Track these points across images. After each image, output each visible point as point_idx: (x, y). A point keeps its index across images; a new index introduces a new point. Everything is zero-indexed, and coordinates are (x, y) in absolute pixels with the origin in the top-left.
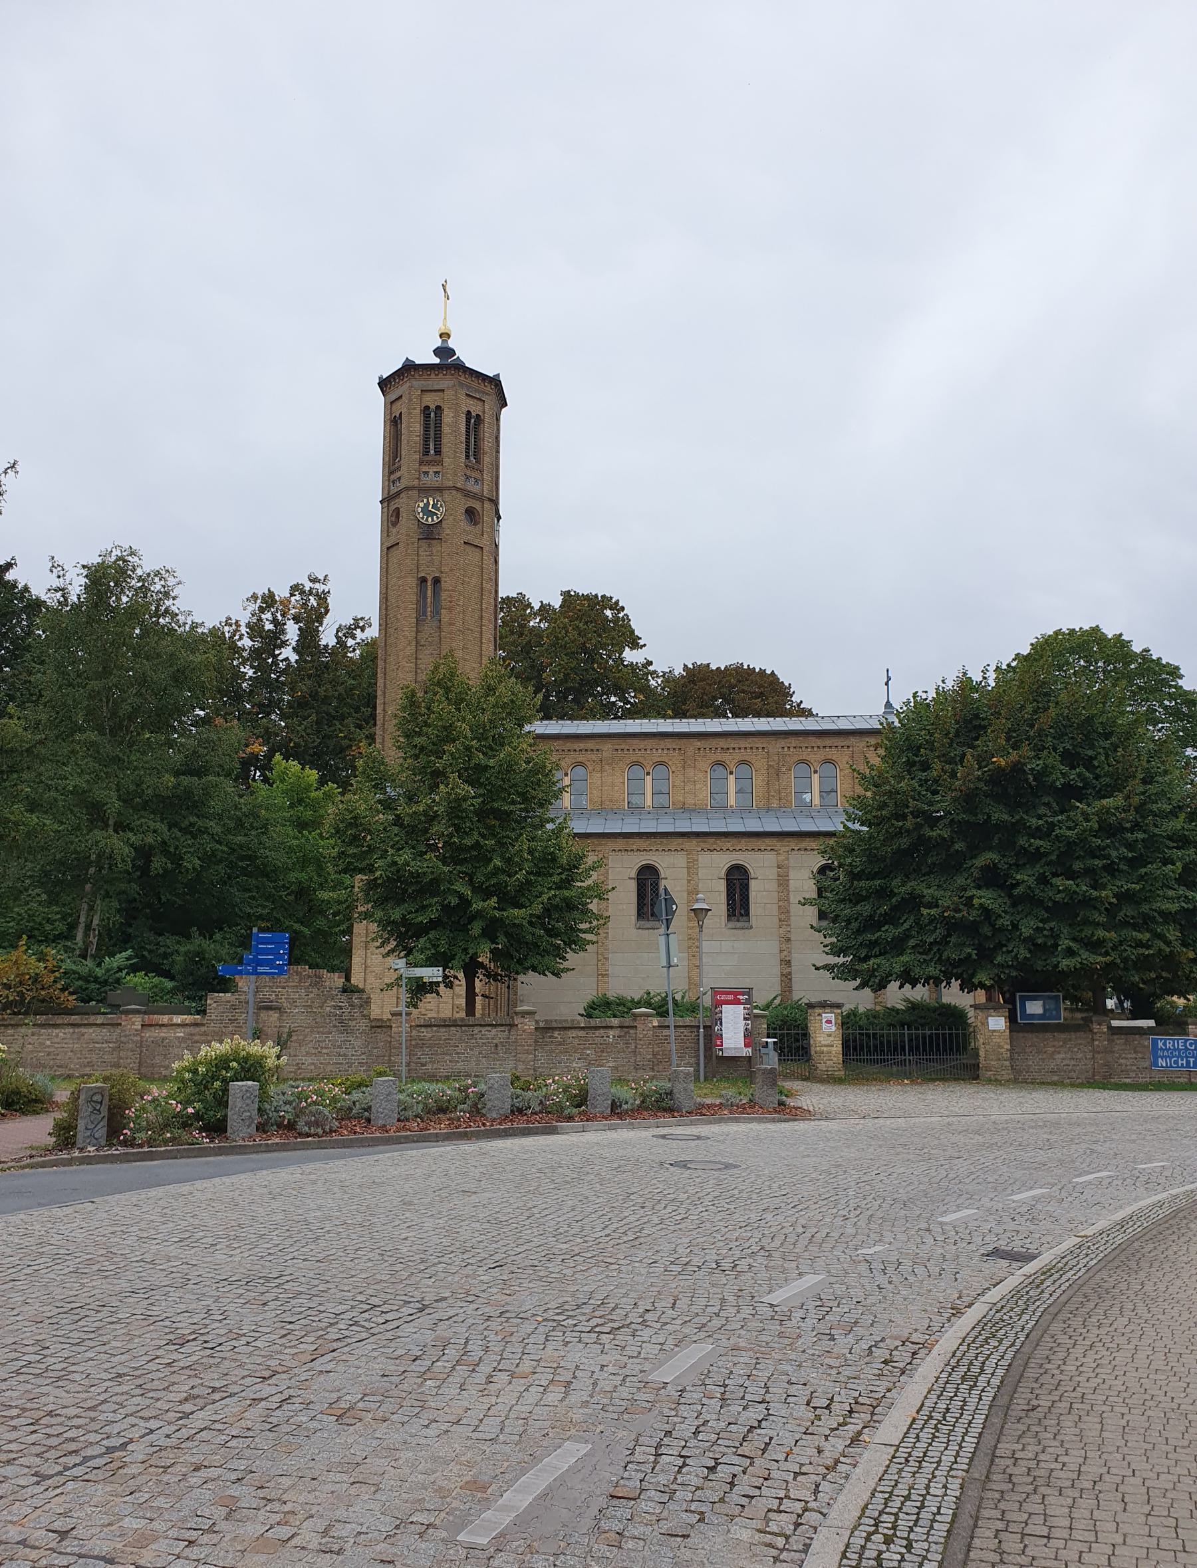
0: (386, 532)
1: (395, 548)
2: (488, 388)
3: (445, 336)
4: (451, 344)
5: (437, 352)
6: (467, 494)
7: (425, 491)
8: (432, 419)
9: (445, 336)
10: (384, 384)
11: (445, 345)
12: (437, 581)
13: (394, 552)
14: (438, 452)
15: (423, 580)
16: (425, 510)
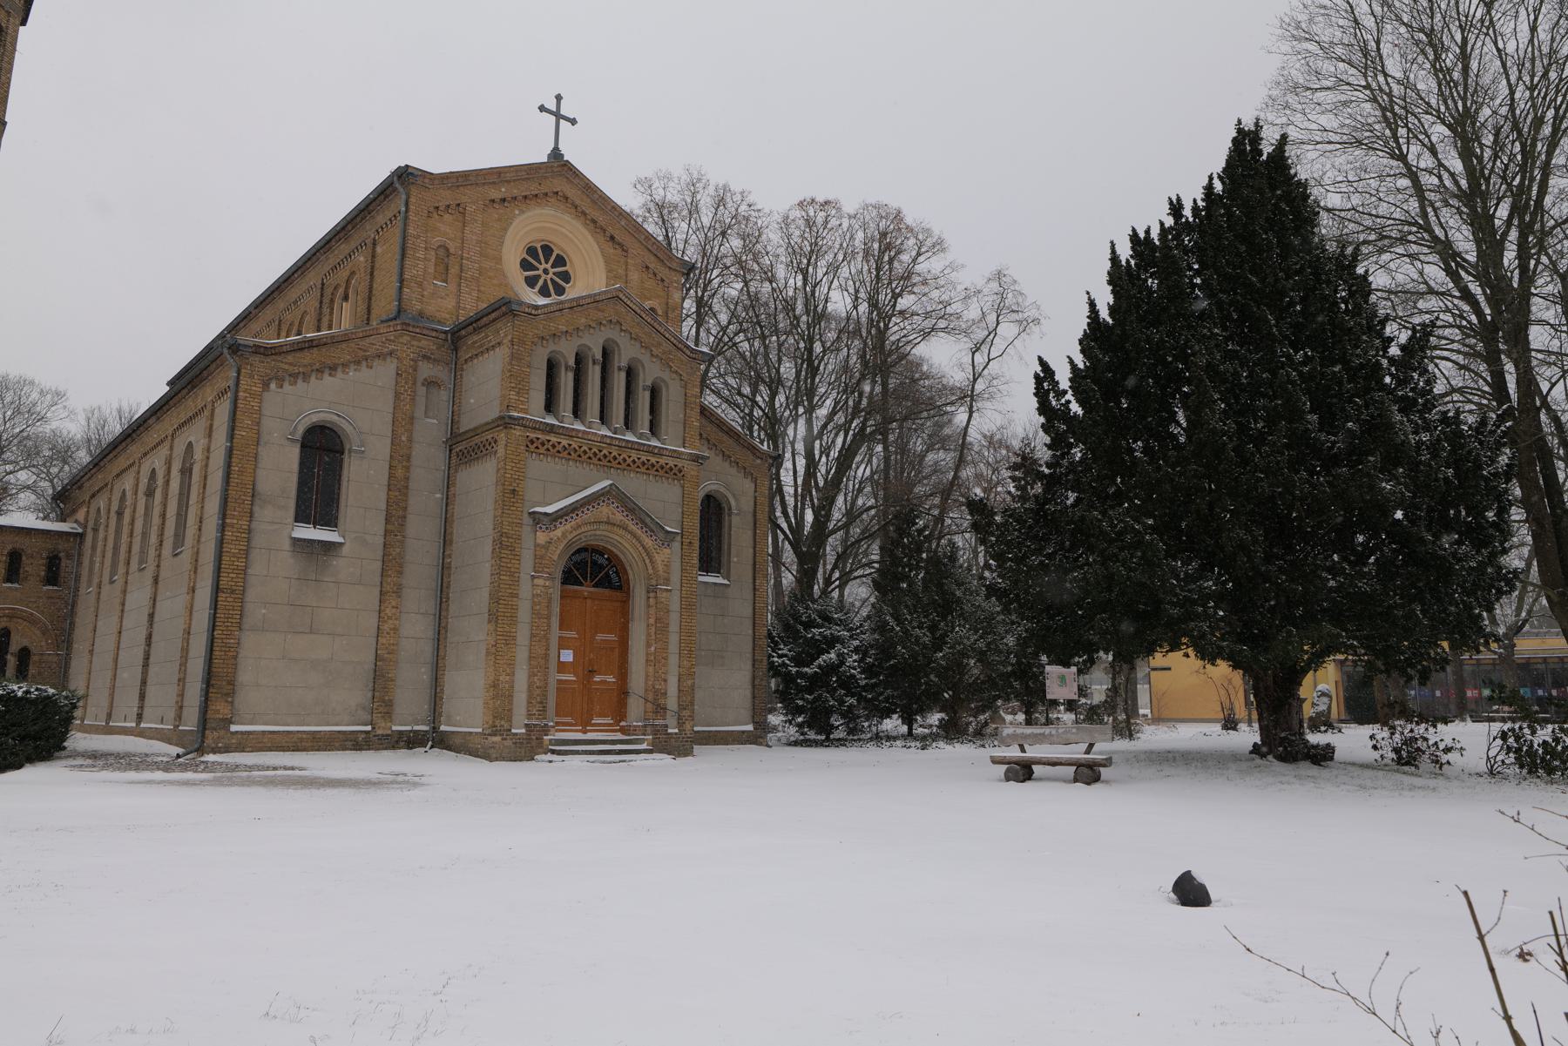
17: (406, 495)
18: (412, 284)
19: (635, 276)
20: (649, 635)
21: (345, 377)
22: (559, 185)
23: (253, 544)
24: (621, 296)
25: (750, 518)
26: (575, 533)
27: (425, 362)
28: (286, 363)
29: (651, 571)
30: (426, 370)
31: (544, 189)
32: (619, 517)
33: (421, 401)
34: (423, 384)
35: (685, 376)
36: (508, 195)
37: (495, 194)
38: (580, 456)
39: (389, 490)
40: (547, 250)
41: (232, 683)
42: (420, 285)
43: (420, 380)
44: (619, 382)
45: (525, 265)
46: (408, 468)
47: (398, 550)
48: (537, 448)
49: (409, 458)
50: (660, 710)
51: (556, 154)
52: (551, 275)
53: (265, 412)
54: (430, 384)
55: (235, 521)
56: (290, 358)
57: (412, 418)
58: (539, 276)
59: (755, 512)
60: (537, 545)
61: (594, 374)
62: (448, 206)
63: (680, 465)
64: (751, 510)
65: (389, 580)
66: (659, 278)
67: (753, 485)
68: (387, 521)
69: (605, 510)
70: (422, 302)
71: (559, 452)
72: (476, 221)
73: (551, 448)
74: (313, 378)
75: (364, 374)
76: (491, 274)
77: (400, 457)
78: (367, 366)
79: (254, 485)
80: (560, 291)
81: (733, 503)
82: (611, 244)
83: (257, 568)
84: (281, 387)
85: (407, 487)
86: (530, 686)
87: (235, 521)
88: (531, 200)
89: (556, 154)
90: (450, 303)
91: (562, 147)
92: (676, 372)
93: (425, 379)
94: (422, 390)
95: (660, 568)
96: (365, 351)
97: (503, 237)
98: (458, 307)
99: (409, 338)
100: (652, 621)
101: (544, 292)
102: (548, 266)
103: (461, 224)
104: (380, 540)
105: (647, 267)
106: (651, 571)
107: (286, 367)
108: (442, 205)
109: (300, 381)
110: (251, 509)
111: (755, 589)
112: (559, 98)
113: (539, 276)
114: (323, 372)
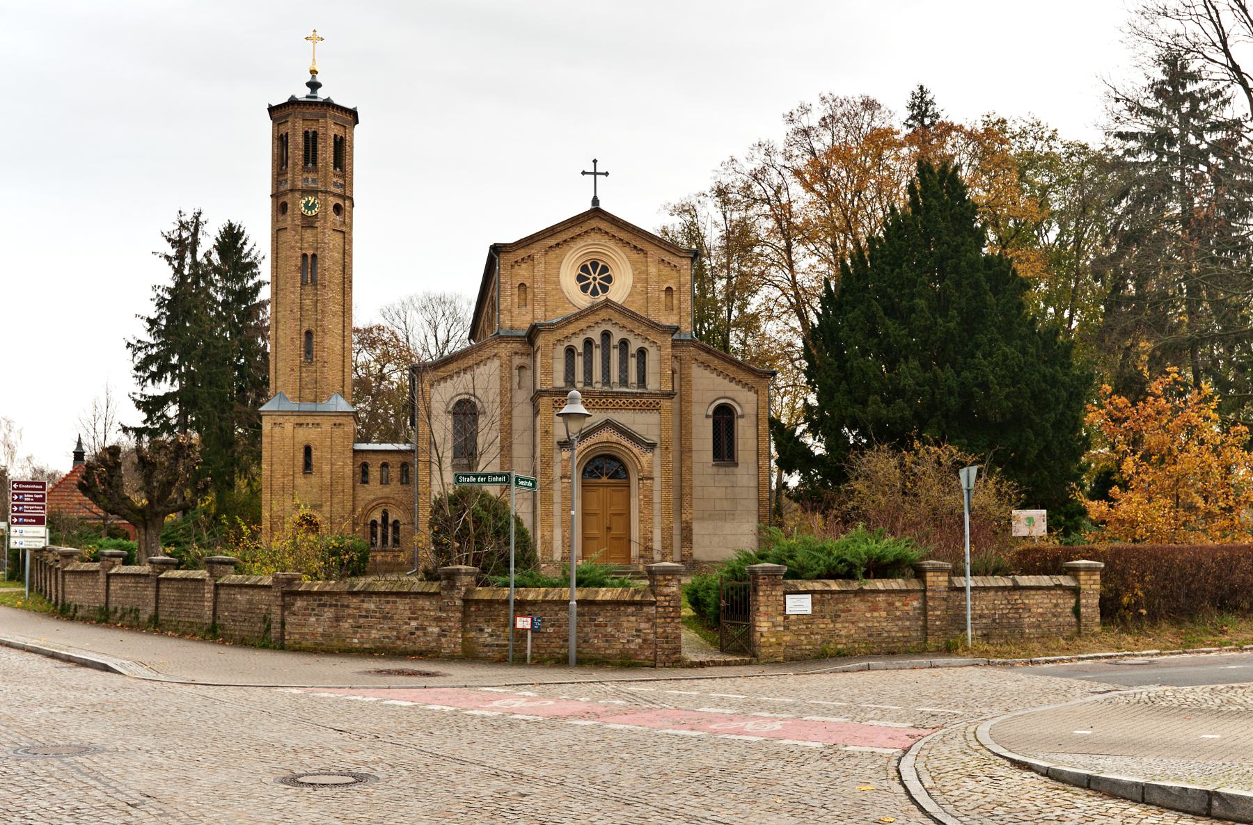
0: (275, 220)
3: (314, 72)
4: (319, 79)
5: (308, 84)
6: (335, 195)
7: (305, 192)
8: (311, 140)
9: (314, 72)
10: (272, 110)
12: (314, 256)
14: (315, 163)
15: (305, 256)
16: (306, 205)
17: (511, 434)
19: (653, 270)
20: (640, 505)
22: (594, 223)
25: (754, 418)
30: (517, 361)
31: (584, 229)
32: (615, 437)
33: (516, 379)
37: (552, 242)
40: (595, 264)
42: (510, 311)
43: (514, 366)
44: (615, 355)
45: (580, 278)
46: (511, 419)
49: (510, 413)
50: (648, 549)
51: (595, 201)
54: (521, 368)
56: (442, 369)
61: (597, 355)
62: (523, 259)
64: (755, 412)
69: (607, 435)
77: (508, 414)
80: (605, 289)
86: (563, 536)
89: (595, 201)
94: (516, 372)
97: (559, 268)
98: (534, 319)
100: (641, 497)
101: (595, 293)
111: (758, 467)
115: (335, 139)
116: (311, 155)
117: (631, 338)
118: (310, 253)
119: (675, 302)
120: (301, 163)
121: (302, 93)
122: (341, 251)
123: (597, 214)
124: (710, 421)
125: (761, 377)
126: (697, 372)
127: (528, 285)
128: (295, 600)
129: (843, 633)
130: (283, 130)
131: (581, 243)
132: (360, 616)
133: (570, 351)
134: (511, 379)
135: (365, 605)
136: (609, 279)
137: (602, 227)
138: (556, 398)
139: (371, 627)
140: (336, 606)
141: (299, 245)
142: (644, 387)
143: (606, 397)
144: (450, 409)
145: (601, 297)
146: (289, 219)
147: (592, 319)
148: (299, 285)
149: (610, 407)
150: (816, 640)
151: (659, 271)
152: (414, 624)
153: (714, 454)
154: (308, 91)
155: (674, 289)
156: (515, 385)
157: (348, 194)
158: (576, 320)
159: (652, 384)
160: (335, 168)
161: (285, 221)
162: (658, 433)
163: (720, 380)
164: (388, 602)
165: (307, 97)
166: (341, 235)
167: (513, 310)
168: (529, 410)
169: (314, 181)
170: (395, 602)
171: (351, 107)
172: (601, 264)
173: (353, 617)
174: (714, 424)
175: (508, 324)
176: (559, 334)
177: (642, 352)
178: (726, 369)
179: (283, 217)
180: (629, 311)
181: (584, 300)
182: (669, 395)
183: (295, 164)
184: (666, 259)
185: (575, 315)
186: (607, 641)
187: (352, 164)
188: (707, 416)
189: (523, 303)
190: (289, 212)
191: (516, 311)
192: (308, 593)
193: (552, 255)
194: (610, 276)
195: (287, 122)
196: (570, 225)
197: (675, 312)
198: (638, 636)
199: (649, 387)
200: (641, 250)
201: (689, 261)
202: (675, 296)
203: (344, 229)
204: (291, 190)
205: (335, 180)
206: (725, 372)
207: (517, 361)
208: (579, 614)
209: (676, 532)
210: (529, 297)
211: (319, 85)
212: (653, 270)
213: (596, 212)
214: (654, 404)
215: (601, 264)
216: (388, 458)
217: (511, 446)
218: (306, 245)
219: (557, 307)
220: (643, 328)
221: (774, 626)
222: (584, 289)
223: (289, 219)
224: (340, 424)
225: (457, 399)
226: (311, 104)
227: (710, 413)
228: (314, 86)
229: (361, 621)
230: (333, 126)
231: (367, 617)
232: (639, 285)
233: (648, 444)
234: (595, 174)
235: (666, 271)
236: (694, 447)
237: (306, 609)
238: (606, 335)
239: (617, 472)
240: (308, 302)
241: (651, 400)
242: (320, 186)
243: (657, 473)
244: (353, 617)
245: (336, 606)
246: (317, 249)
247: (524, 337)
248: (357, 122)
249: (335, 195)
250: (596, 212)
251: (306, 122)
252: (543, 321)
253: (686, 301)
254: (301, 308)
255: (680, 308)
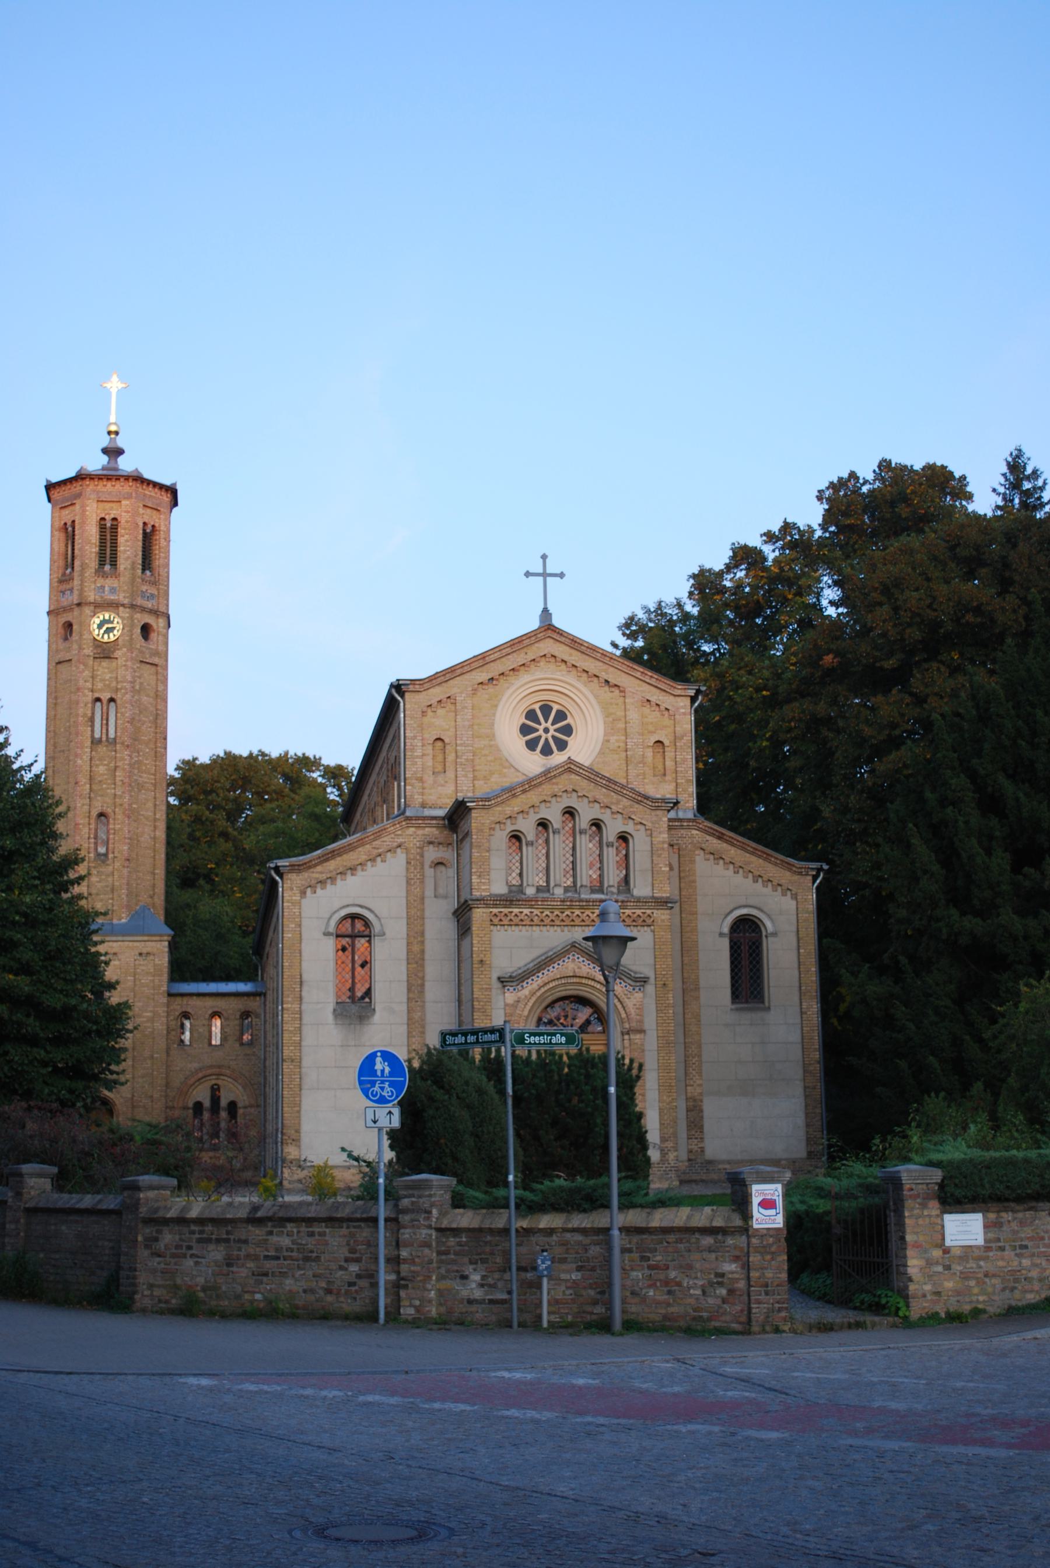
1: (66, 665)
2: (166, 498)
4: (121, 442)
5: (105, 451)
6: (143, 609)
8: (109, 532)
10: (50, 487)
11: (112, 445)
13: (62, 668)
14: (114, 563)
17: (423, 966)
18: (414, 781)
21: (364, 873)
22: (548, 646)
23: (304, 1021)
24: (572, 767)
26: (543, 990)
27: (431, 846)
28: (317, 872)
29: (624, 1015)
30: (432, 854)
31: (531, 657)
34: (431, 867)
35: (649, 825)
36: (494, 674)
37: (483, 676)
38: (542, 920)
39: (408, 963)
40: (546, 709)
41: (298, 1131)
42: (421, 780)
45: (525, 730)
46: (423, 942)
47: (419, 1014)
48: (501, 920)
49: (422, 934)
51: (546, 613)
52: (552, 732)
53: (303, 915)
55: (289, 1006)
56: (319, 868)
57: (423, 898)
58: (540, 737)
59: (798, 931)
60: (506, 1005)
63: (649, 912)
64: (794, 929)
65: (414, 1040)
66: (662, 708)
67: (794, 903)
68: (409, 990)
70: (423, 794)
71: (522, 920)
72: (466, 707)
73: (512, 918)
74: (339, 881)
75: (379, 867)
76: (486, 752)
77: (416, 936)
78: (382, 861)
79: (301, 975)
80: (562, 746)
81: (768, 924)
82: (607, 688)
83: (309, 1038)
84: (315, 892)
85: (423, 959)
87: (289, 1006)
88: (518, 670)
89: (546, 613)
90: (450, 789)
91: (549, 607)
92: (641, 823)
93: (432, 862)
94: (429, 872)
95: (632, 1011)
96: (378, 849)
97: (494, 715)
98: (457, 791)
99: (412, 829)
101: (547, 751)
102: (544, 725)
103: (454, 714)
104: (404, 1007)
105: (648, 701)
106: (624, 1015)
107: (317, 875)
108: (434, 701)
109: (329, 886)
110: (301, 995)
111: (802, 1013)
112: (544, 557)
113: (540, 737)
114: (345, 874)
115: (144, 530)
116: (108, 554)
117: (606, 816)
118: (105, 696)
119: (669, 763)
120: (93, 564)
121: (97, 462)
122: (152, 694)
123: (549, 633)
124: (726, 943)
125: (800, 874)
126: (703, 866)
127: (447, 740)
128: (159, 1232)
129: (1034, 1274)
130: (67, 516)
131: (525, 677)
132: (266, 1257)
133: (516, 837)
134: (422, 882)
135: (274, 1239)
136: (568, 730)
137: (556, 654)
138: (495, 911)
139: (283, 1275)
140: (227, 1241)
141: (89, 685)
142: (628, 890)
143: (570, 907)
144: (332, 928)
145: (558, 758)
146: (75, 646)
147: (547, 789)
148: (88, 743)
149: (577, 923)
150: (994, 1286)
151: (643, 716)
152: (354, 1268)
153: (733, 993)
154: (104, 459)
155: (666, 742)
156: (429, 892)
157: (162, 609)
158: (524, 791)
159: (641, 888)
160: (144, 570)
161: (69, 649)
162: (652, 962)
163: (739, 879)
164: (311, 1234)
165: (103, 469)
166: (153, 669)
167: (425, 777)
168: (450, 928)
169: (113, 590)
170: (322, 1234)
171: (167, 482)
172: (555, 707)
173: (255, 1258)
174: (731, 947)
175: (418, 799)
176: (498, 812)
177: (623, 838)
178: (749, 863)
179: (67, 644)
180: (603, 777)
181: (533, 763)
182: (663, 903)
183: (83, 567)
184: (653, 699)
185: (522, 784)
186: (669, 1292)
187: (167, 565)
188: (721, 935)
189: (440, 768)
190: (75, 636)
191: (429, 779)
192: (182, 1221)
193: (483, 694)
194: (569, 726)
195: (74, 504)
196: (509, 650)
197: (668, 778)
198: (721, 1284)
199: (636, 892)
200: (616, 685)
201: (688, 701)
202: (669, 754)
203: (156, 660)
204: (79, 605)
205: (144, 588)
206: (747, 868)
207: (432, 854)
208: (624, 1250)
209: (682, 1114)
210: (451, 757)
211: (120, 452)
212: (633, 715)
213: (548, 628)
214: (644, 917)
215: (555, 707)
216: (220, 1004)
217: (423, 985)
218: (100, 685)
219: (492, 773)
220: (625, 802)
221: (930, 1263)
222: (531, 745)
223: (75, 646)
224: (148, 954)
225: (343, 913)
226: (110, 476)
227: (726, 930)
228: (113, 452)
229: (269, 1265)
230: (141, 511)
231: (278, 1258)
232: (613, 739)
233: (636, 980)
234: (545, 575)
235: (653, 716)
236: (702, 983)
237: (178, 1247)
238: (570, 813)
239: (588, 1022)
240: (102, 769)
241: (639, 912)
242: (122, 597)
243: (650, 1022)
244: (255, 1258)
245: (227, 1241)
246: (117, 690)
247: (443, 818)
248: (175, 504)
249: (143, 609)
250: (548, 628)
251: (101, 505)
252: (470, 795)
253: (684, 760)
254: (91, 778)
255: (676, 772)
